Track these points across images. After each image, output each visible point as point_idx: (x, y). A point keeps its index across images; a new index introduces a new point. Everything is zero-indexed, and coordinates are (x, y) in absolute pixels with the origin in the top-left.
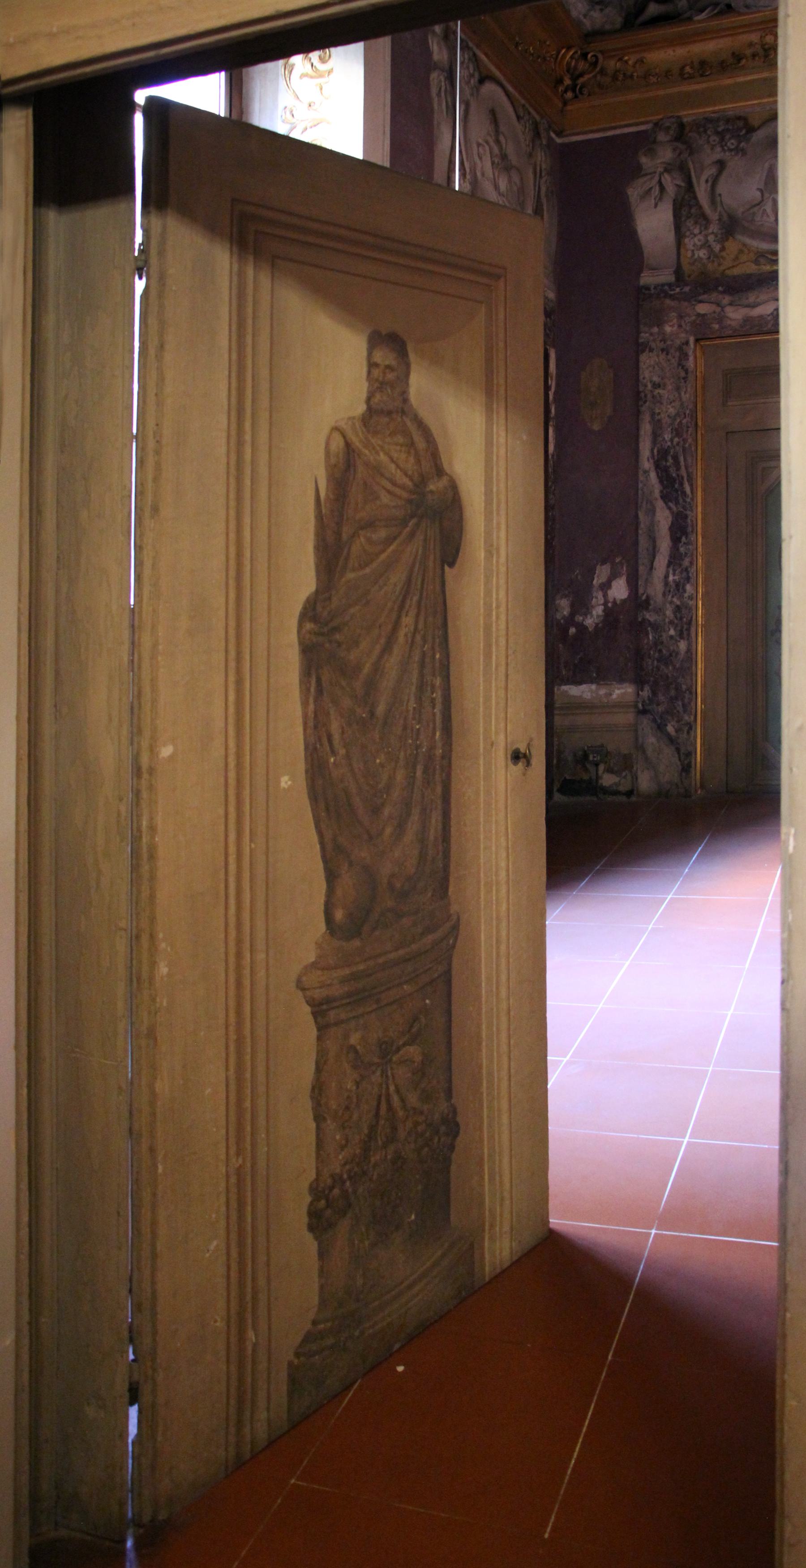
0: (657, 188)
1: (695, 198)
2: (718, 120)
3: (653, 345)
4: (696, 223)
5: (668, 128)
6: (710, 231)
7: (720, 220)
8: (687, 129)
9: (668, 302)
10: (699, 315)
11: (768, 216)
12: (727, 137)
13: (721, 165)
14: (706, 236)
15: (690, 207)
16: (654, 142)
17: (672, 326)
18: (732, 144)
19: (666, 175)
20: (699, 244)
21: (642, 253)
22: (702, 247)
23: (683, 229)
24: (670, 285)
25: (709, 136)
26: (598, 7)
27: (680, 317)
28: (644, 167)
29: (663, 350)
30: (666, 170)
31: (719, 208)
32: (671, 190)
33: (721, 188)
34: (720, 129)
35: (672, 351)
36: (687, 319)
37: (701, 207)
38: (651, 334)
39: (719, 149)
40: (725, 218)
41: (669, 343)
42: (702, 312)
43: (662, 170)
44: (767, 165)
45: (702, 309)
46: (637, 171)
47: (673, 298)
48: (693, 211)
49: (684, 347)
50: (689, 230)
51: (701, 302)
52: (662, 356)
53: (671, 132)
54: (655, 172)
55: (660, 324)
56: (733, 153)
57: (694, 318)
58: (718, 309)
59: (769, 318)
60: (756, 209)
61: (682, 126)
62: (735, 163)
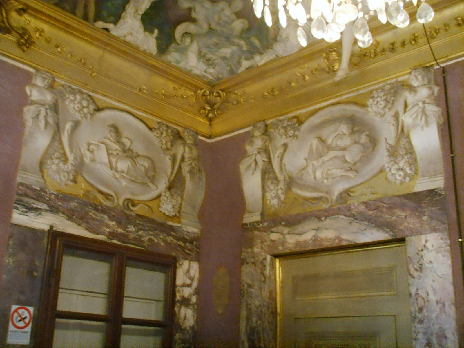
0: (254, 163)
1: (272, 168)
2: (284, 120)
3: (248, 260)
4: (272, 183)
5: (260, 127)
6: (279, 187)
7: (284, 180)
8: (269, 127)
9: (256, 232)
10: (272, 241)
11: (310, 175)
12: (289, 129)
13: (285, 145)
14: (277, 190)
15: (270, 173)
16: (253, 137)
17: (258, 248)
18: (291, 133)
19: (258, 155)
20: (273, 195)
21: (245, 203)
22: (275, 197)
23: (266, 187)
24: (257, 222)
25: (279, 130)
26: (211, 67)
27: (262, 242)
28: (248, 152)
29: (253, 263)
30: (259, 153)
31: (284, 173)
32: (261, 164)
33: (285, 160)
34: (285, 125)
35: (258, 263)
36: (265, 244)
37: (275, 173)
38: (247, 253)
39: (284, 137)
40: (287, 179)
41: (257, 258)
42: (273, 239)
43: (256, 152)
44: (309, 144)
45: (274, 236)
46: (244, 154)
47: (258, 230)
48: (271, 175)
49: (264, 261)
50: (269, 187)
51: (272, 232)
52: (253, 266)
53: (261, 130)
54: (253, 154)
55: (251, 246)
56: (292, 139)
57: (269, 243)
58: (282, 237)
59: (310, 242)
60: (303, 171)
61: (266, 126)
62: (293, 144)
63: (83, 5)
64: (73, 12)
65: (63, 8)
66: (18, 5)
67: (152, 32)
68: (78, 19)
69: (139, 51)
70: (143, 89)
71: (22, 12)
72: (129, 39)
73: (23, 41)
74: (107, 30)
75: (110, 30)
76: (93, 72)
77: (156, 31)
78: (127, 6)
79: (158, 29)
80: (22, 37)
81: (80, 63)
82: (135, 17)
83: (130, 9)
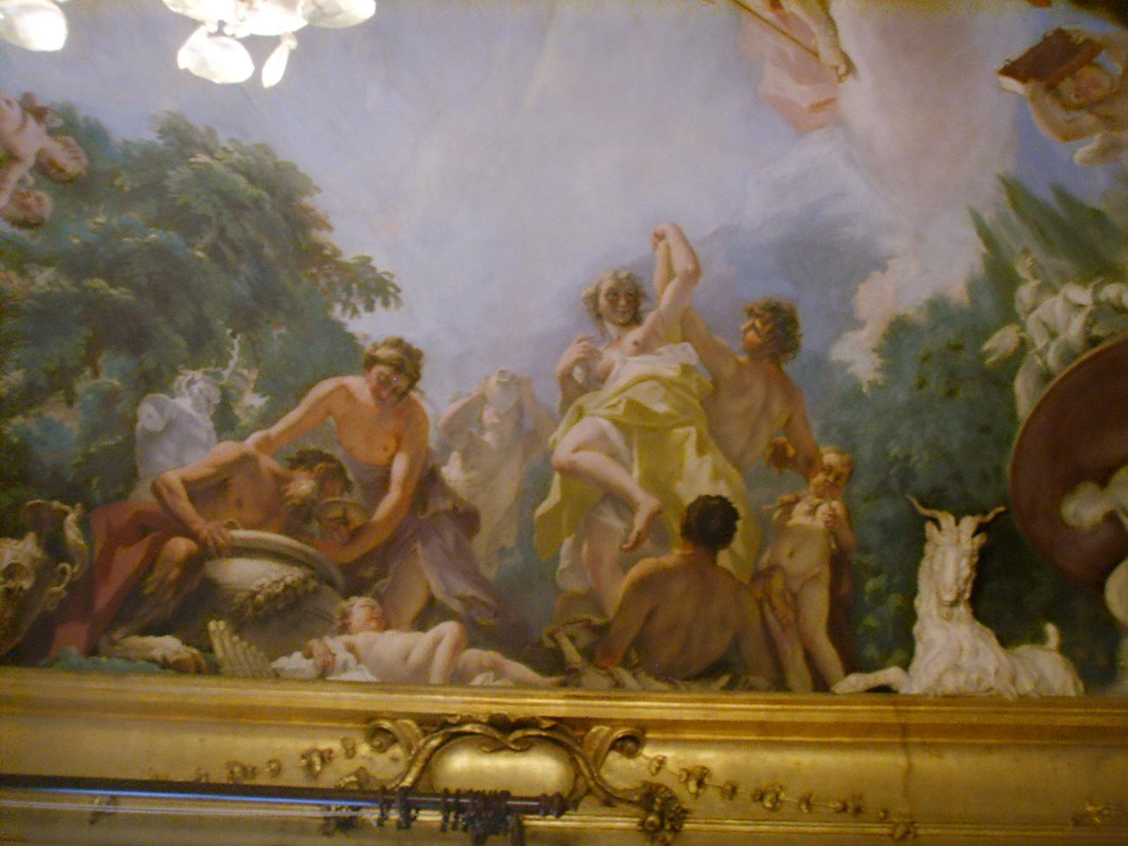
63: (799, 655)
64: (780, 683)
65: (751, 689)
66: (611, 733)
67: (1038, 638)
68: (803, 697)
69: (1009, 704)
70: (1087, 815)
71: (630, 745)
72: (951, 684)
73: (651, 818)
74: (885, 689)
75: (894, 688)
76: (893, 825)
77: (1051, 630)
78: (917, 602)
79: (1051, 618)
80: (649, 810)
81: (845, 815)
82: (949, 618)
83: (926, 604)
